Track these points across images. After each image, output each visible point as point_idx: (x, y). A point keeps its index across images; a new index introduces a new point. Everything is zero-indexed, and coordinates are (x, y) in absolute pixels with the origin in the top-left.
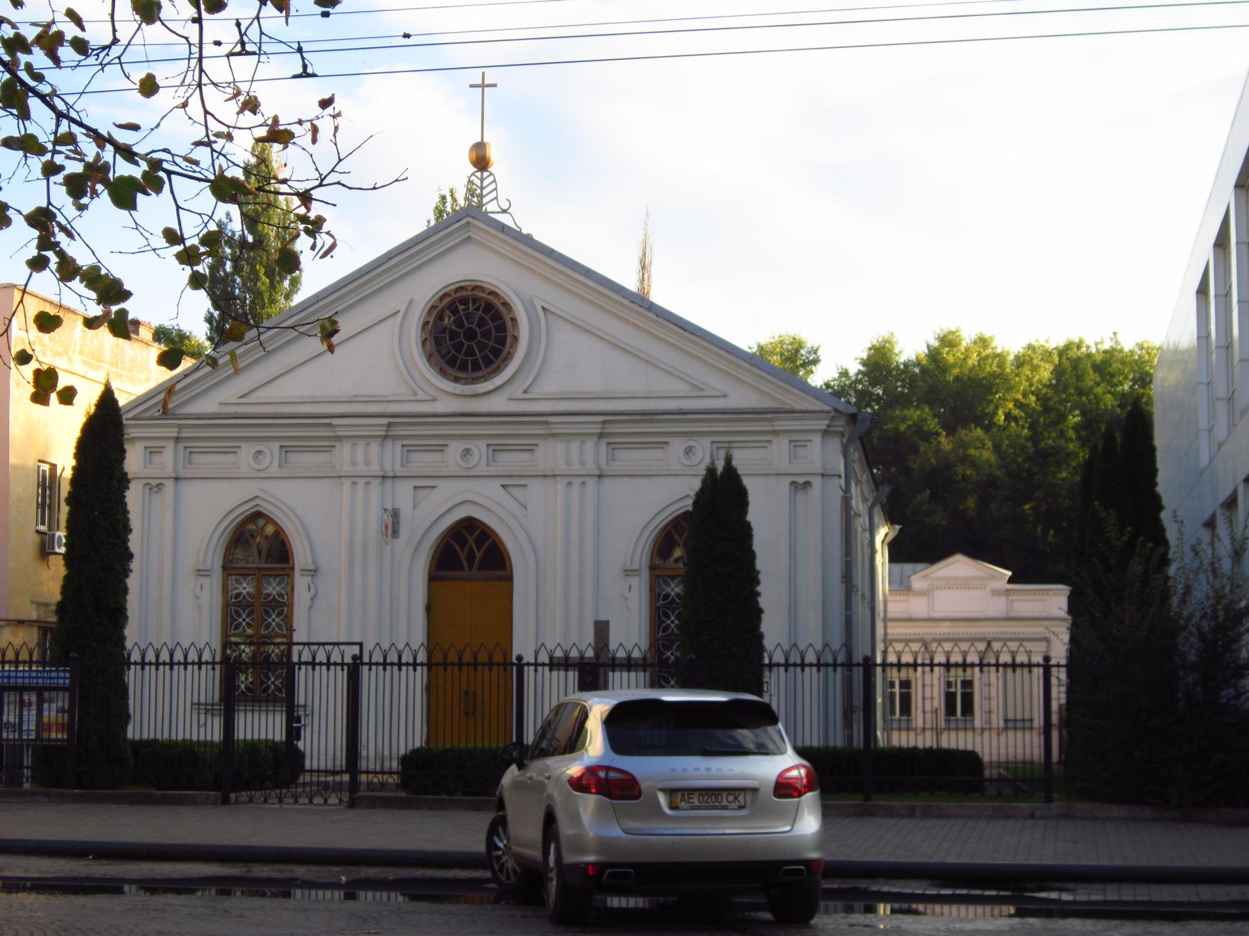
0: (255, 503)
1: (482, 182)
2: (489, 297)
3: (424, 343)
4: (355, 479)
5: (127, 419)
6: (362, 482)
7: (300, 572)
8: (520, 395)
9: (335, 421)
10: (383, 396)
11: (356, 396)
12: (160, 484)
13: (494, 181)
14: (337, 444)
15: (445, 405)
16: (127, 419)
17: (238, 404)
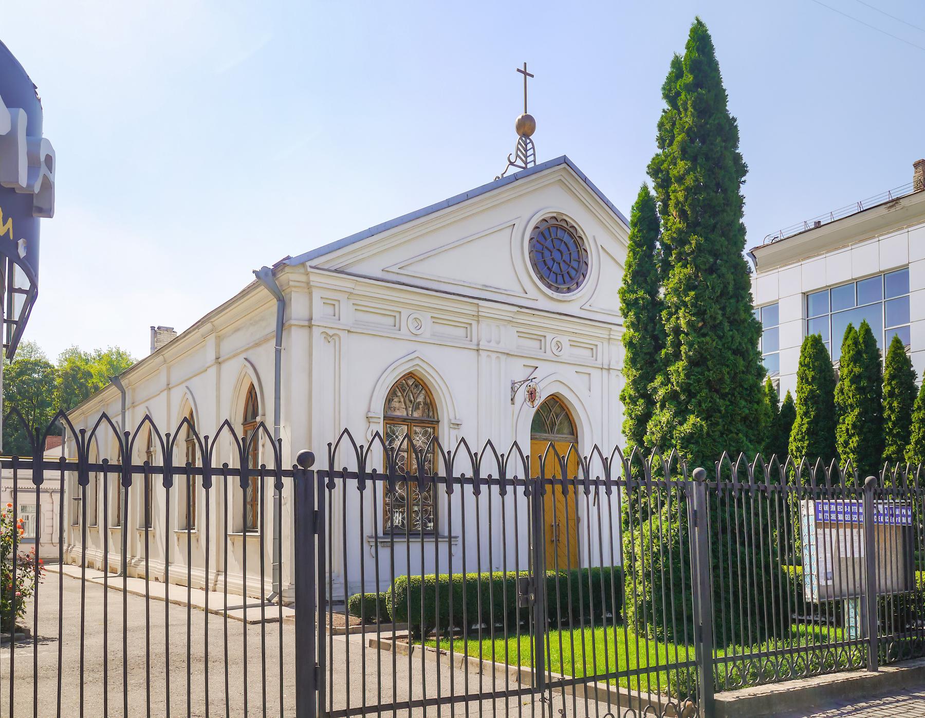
0: (417, 362)
1: (526, 146)
2: (571, 229)
3: (530, 254)
4: (489, 353)
5: (311, 267)
6: (494, 355)
7: (452, 426)
8: (587, 307)
9: (481, 303)
10: (505, 290)
11: (487, 286)
12: (334, 335)
13: (533, 148)
14: (474, 324)
15: (543, 304)
16: (311, 267)
17: (398, 273)
